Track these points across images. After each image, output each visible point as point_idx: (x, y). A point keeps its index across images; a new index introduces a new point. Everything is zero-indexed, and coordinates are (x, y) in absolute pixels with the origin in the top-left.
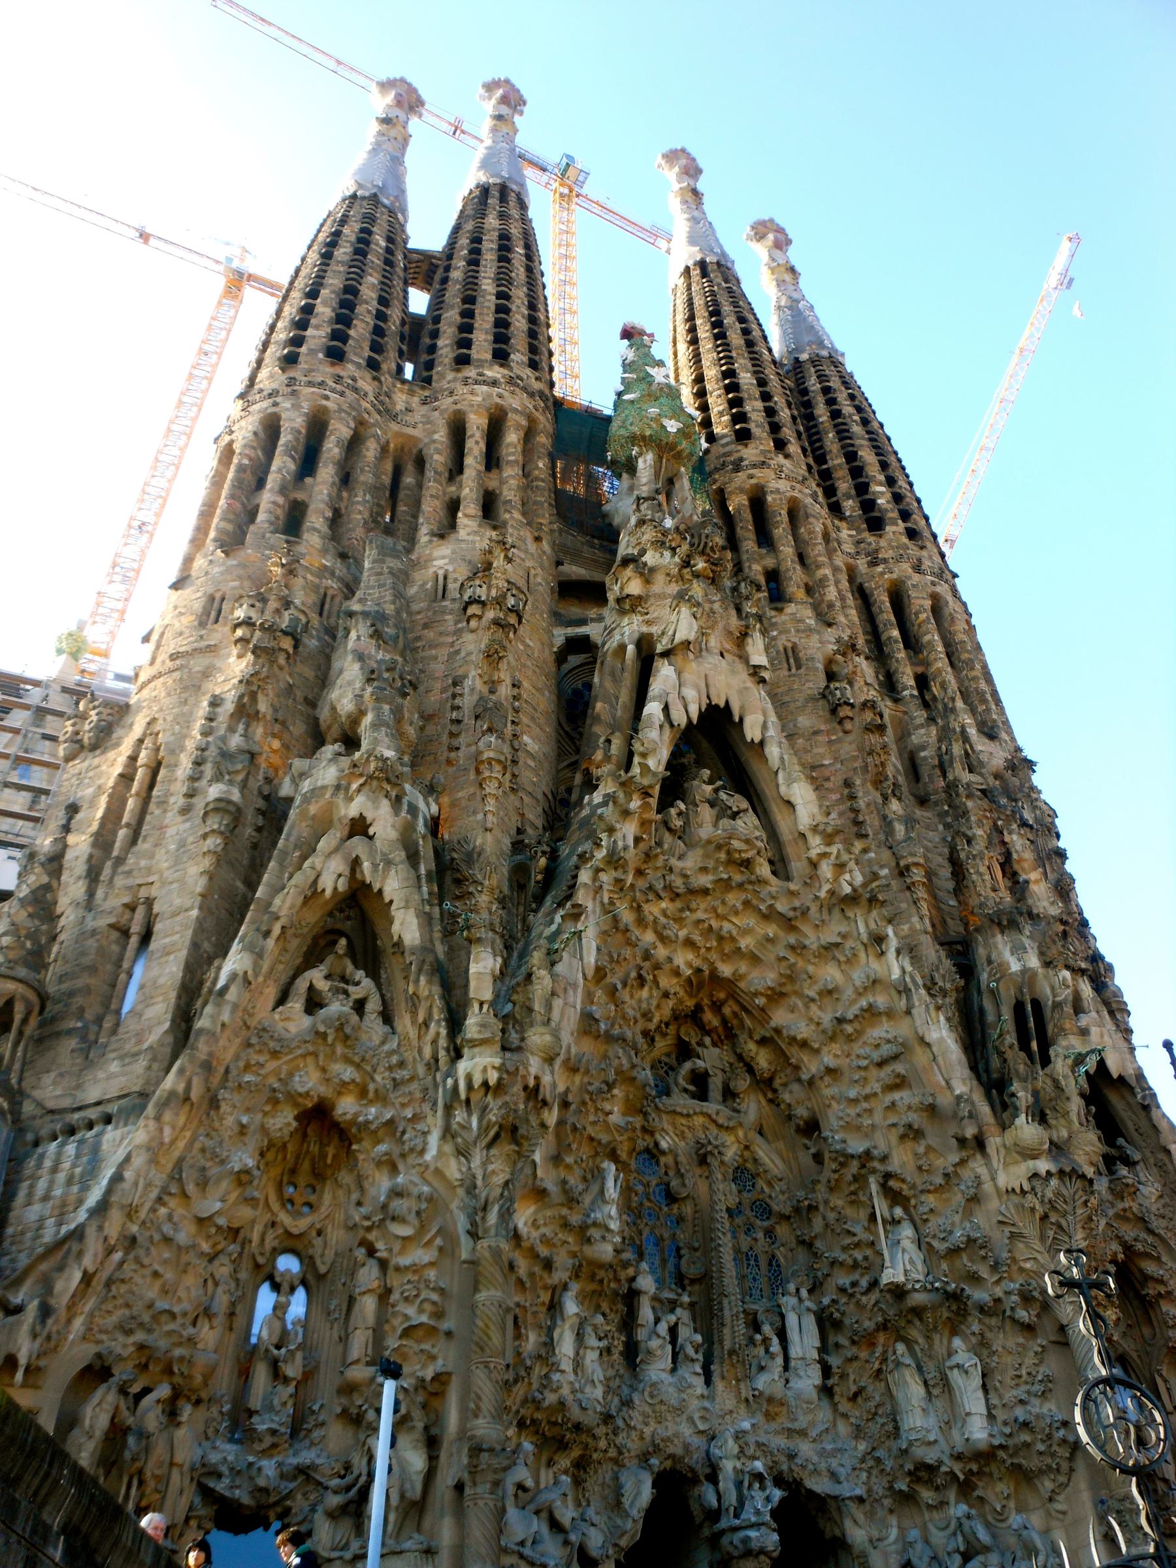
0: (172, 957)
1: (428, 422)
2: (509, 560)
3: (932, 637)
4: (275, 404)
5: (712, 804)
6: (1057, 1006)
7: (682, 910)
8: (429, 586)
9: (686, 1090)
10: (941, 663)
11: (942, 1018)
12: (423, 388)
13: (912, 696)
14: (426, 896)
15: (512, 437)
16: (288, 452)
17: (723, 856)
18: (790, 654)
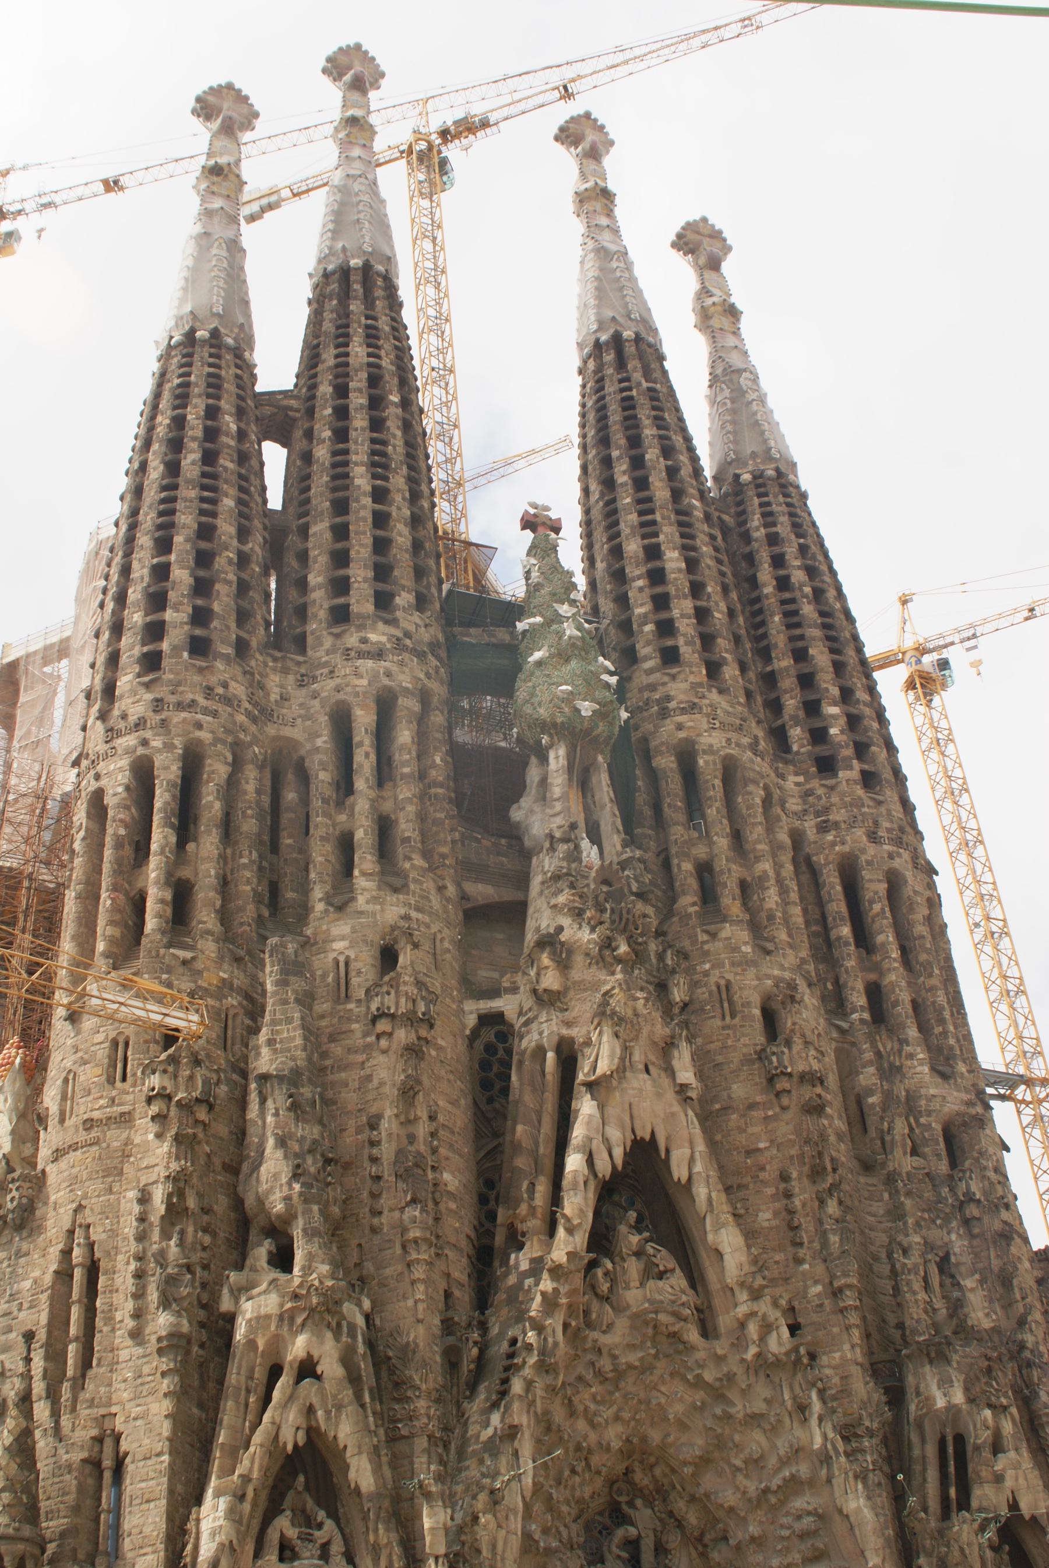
0: (152, 1505)
1: (306, 717)
2: (416, 946)
3: (886, 937)
4: (145, 743)
5: (639, 1254)
6: (977, 1448)
7: (611, 1393)
8: (330, 979)
9: (619, 1557)
10: (895, 977)
11: (860, 1486)
12: (299, 664)
13: (862, 1020)
14: (373, 1428)
15: (404, 736)
16: (167, 823)
17: (650, 1331)
18: (724, 996)
